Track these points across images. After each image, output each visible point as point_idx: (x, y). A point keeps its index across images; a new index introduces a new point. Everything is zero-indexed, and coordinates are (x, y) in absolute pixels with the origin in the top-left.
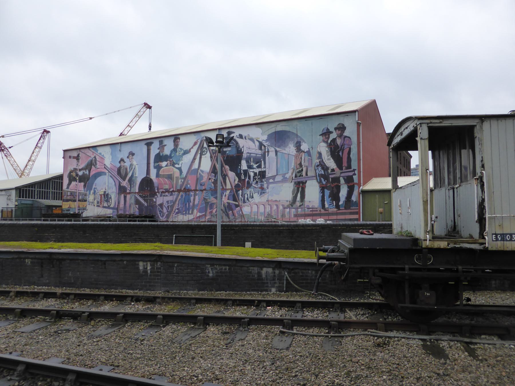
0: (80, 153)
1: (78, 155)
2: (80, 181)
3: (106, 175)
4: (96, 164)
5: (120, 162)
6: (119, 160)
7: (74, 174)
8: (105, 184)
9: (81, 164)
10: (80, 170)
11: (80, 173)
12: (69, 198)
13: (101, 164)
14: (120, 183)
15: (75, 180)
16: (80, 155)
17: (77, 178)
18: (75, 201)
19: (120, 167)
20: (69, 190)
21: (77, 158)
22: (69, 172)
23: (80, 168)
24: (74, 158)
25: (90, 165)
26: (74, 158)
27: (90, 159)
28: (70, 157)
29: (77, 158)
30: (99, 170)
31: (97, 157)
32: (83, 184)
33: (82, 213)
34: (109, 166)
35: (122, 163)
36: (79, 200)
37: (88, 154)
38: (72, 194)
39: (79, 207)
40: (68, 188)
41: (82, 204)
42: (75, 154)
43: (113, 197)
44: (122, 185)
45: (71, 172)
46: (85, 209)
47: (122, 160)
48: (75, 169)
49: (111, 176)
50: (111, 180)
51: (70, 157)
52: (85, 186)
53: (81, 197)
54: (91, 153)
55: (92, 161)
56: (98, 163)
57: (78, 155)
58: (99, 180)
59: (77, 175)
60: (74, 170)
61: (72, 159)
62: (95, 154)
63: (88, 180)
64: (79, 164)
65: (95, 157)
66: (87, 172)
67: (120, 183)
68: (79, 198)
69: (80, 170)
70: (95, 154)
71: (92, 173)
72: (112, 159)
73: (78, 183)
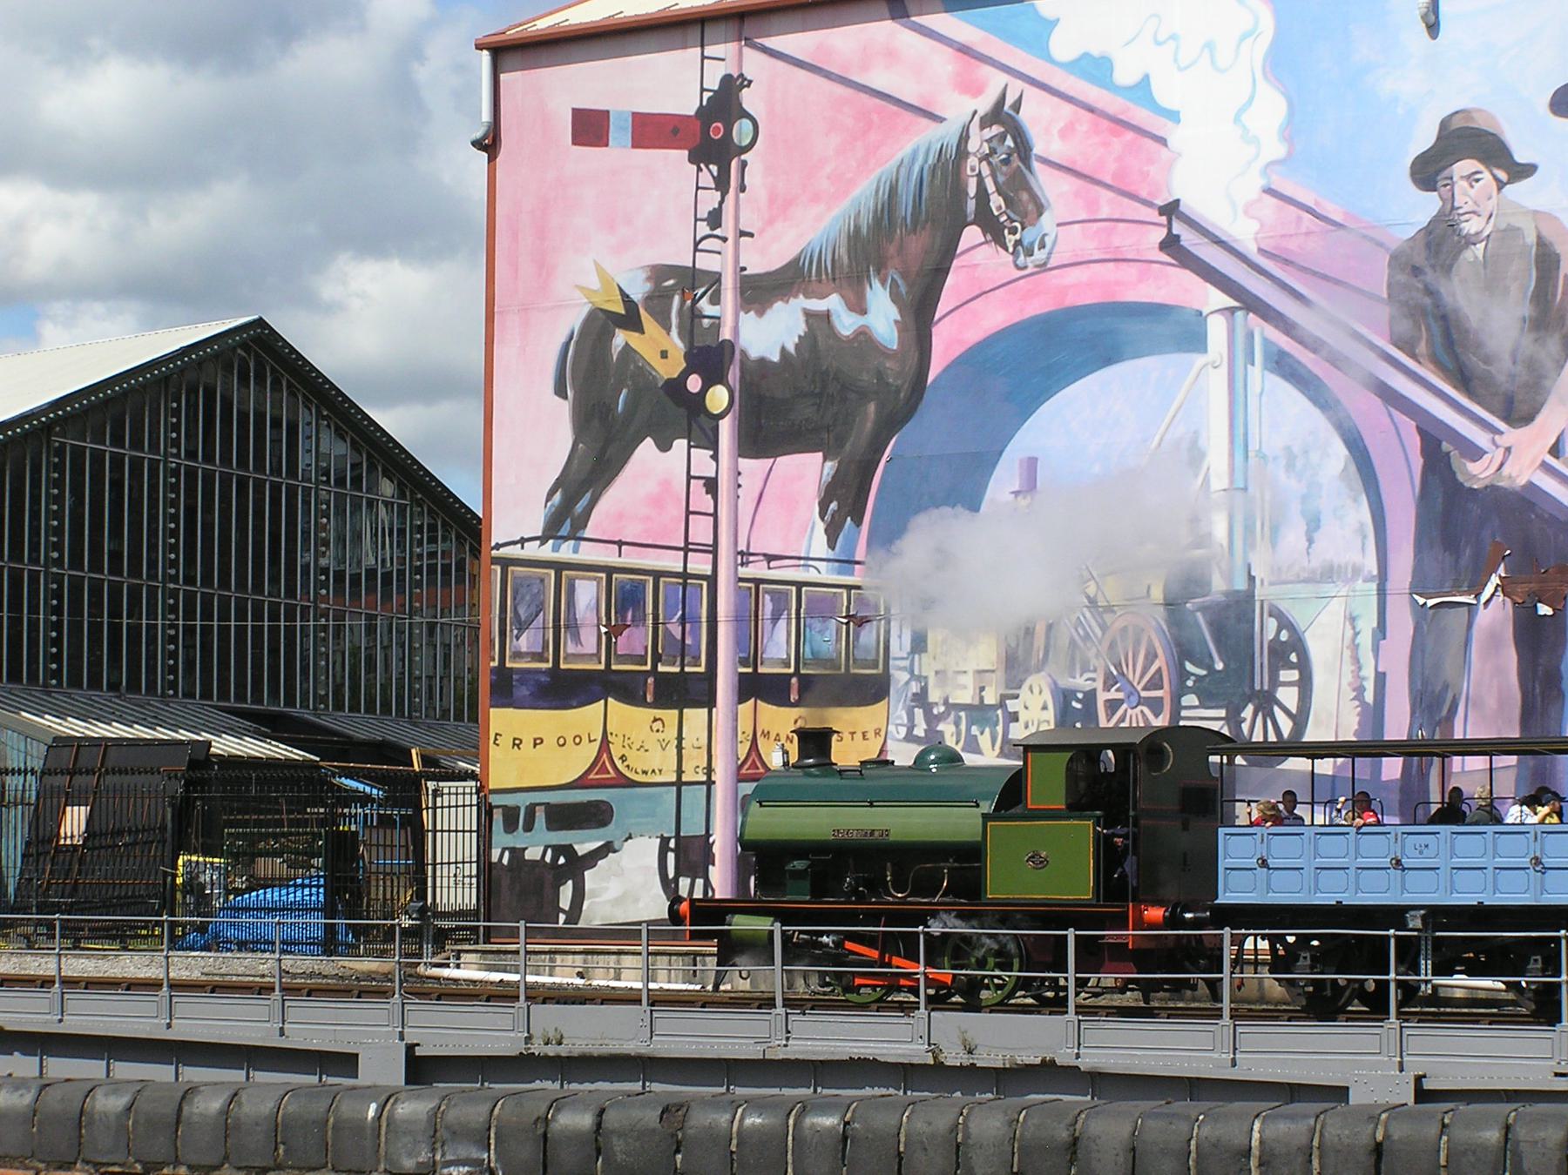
0: (754, 64)
1: (725, 101)
2: (763, 437)
3: (1191, 337)
4: (1024, 202)
5: (1428, 172)
6: (1425, 138)
7: (660, 350)
8: (1196, 456)
9: (780, 206)
10: (759, 292)
11: (769, 334)
12: (584, 649)
13: (1108, 204)
14: (1438, 451)
15: (679, 415)
16: (749, 99)
17: (718, 398)
18: (686, 691)
19: (1442, 239)
20: (589, 553)
21: (711, 136)
22: (574, 319)
23: (762, 259)
24: (652, 131)
25: (921, 227)
26: (652, 131)
27: (947, 134)
28: (590, 128)
29: (711, 136)
30: (1078, 287)
31: (1037, 115)
32: (807, 470)
34: (1245, 234)
35: (1471, 183)
36: (755, 687)
37: (879, 81)
38: (626, 596)
40: (566, 519)
42: (673, 81)
43: (1322, 647)
44: (1477, 473)
45: (600, 325)
47: (1468, 141)
48: (680, 286)
49: (1282, 365)
50: (1285, 414)
51: (590, 128)
52: (845, 500)
53: (778, 647)
54: (943, 62)
55: (950, 165)
56: (1046, 182)
57: (725, 101)
58: (1079, 423)
59: (710, 358)
60: (658, 301)
61: (619, 152)
62: (996, 81)
63: (893, 422)
64: (748, 208)
65: (1002, 116)
66: (882, 316)
67: (1438, 451)
68: (750, 654)
69: (759, 292)
70: (996, 81)
71: (950, 338)
72: (1290, 132)
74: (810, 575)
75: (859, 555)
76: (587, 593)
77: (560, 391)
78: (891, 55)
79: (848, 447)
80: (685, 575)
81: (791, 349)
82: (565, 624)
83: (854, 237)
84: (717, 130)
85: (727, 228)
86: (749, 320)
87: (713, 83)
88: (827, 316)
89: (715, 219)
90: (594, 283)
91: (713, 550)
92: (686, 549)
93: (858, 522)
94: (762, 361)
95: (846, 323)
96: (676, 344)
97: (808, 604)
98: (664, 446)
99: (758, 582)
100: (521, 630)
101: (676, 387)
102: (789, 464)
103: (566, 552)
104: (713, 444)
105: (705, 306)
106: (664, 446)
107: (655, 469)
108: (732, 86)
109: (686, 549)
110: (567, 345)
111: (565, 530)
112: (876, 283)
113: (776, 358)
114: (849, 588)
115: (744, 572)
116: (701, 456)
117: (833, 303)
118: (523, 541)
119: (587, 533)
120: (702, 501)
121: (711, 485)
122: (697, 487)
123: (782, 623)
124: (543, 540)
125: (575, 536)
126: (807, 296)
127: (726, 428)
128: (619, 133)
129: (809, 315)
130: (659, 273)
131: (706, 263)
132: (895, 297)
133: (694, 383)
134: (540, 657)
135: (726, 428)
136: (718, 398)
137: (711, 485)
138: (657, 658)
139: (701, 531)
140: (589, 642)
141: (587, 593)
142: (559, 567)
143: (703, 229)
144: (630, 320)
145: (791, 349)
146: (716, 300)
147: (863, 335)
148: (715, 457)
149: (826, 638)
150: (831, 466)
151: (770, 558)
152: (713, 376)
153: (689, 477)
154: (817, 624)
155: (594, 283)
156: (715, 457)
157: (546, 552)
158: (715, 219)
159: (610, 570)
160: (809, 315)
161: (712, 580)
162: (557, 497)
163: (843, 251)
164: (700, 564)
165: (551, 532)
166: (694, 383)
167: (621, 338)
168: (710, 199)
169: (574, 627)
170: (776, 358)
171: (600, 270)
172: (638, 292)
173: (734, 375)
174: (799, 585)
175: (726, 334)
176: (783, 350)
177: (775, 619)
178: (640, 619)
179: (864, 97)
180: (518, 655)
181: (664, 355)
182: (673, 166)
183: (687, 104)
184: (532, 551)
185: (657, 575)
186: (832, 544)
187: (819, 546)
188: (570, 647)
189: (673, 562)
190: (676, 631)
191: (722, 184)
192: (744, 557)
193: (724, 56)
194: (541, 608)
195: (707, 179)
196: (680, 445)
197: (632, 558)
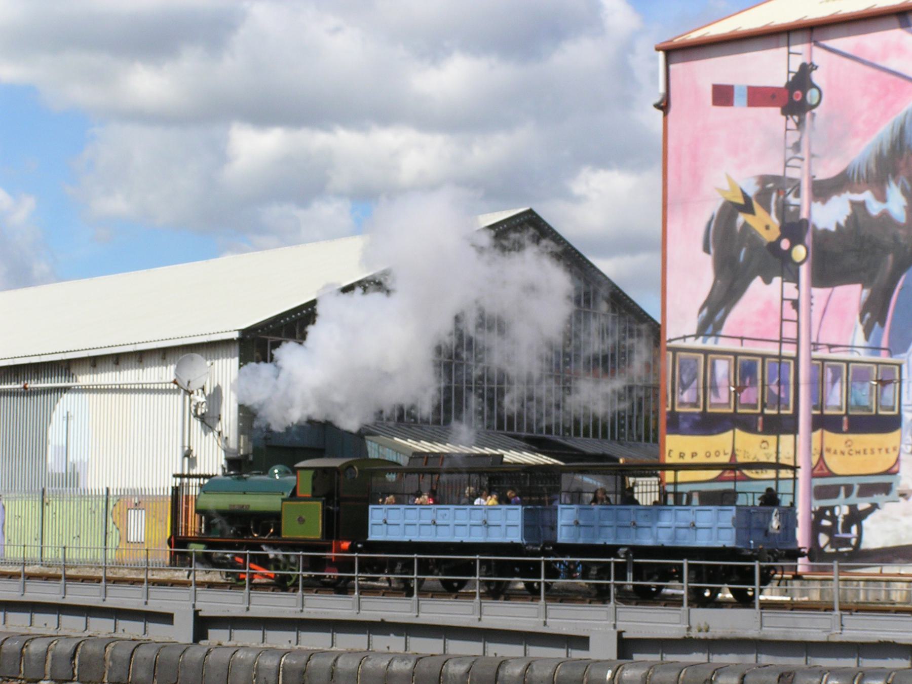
0: (819, 56)
1: (802, 79)
2: (825, 275)
7: (765, 225)
11: (829, 215)
12: (721, 400)
15: (776, 263)
16: (817, 77)
17: (799, 253)
18: (782, 425)
20: (724, 344)
22: (713, 207)
23: (827, 170)
24: (759, 97)
26: (759, 97)
28: (723, 95)
29: (795, 98)
32: (852, 295)
33: (856, 517)
37: (893, 64)
38: (746, 370)
39: (820, 470)
40: (710, 323)
41: (853, 456)
42: (772, 67)
45: (729, 211)
46: (880, 487)
48: (773, 188)
51: (723, 95)
52: (874, 311)
57: (802, 79)
59: (794, 229)
60: (764, 196)
61: (740, 109)
68: (819, 402)
69: (823, 190)
73: (803, 287)
74: (854, 356)
75: (884, 344)
76: (722, 368)
77: (706, 249)
78: (900, 49)
79: (876, 281)
80: (780, 357)
81: (842, 223)
82: (710, 386)
83: (880, 159)
84: (797, 95)
85: (804, 153)
86: (817, 207)
87: (795, 68)
88: (862, 204)
89: (797, 147)
90: (726, 186)
91: (797, 342)
92: (781, 341)
93: (883, 324)
94: (826, 231)
95: (875, 208)
96: (774, 221)
97: (856, 374)
98: (768, 281)
99: (823, 360)
100: (684, 387)
101: (774, 246)
102: (842, 291)
103: (710, 344)
104: (796, 279)
105: (792, 199)
106: (768, 281)
107: (762, 295)
108: (806, 70)
109: (781, 341)
110: (710, 223)
111: (710, 330)
112: (893, 184)
113: (833, 228)
114: (877, 364)
115: (815, 355)
116: (790, 287)
117: (866, 196)
118: (685, 337)
119: (724, 332)
120: (790, 313)
121: (796, 304)
122: (787, 305)
123: (838, 385)
124: (697, 336)
125: (716, 334)
126: (852, 192)
127: (804, 271)
128: (740, 98)
129: (853, 204)
130: (764, 180)
131: (792, 173)
132: (904, 192)
133: (785, 244)
134: (695, 405)
135: (804, 271)
136: (799, 253)
137: (796, 304)
138: (764, 406)
139: (790, 331)
140: (724, 396)
141: (722, 368)
142: (706, 352)
143: (790, 153)
144: (747, 207)
145: (842, 223)
146: (797, 195)
147: (885, 215)
148: (798, 287)
149: (865, 395)
150: (866, 293)
151: (830, 346)
152: (796, 239)
153: (783, 299)
154: (858, 385)
155: (726, 186)
156: (798, 287)
157: (698, 343)
158: (797, 147)
159: (736, 354)
160: (853, 204)
161: (796, 360)
162: (705, 312)
163: (873, 166)
164: (789, 350)
165: (702, 332)
166: (785, 244)
167: (741, 218)
168: (793, 137)
169: (715, 388)
170: (833, 228)
171: (729, 178)
172: (751, 191)
173: (808, 239)
174: (848, 362)
175: (804, 215)
176: (838, 225)
177: (834, 382)
178: (753, 383)
179: (885, 75)
180: (682, 404)
181: (767, 227)
182: (772, 115)
183: (778, 79)
184: (691, 343)
185: (764, 357)
186: (867, 337)
187: (859, 338)
188: (712, 399)
189: (772, 349)
190: (775, 389)
191: (800, 125)
192: (815, 346)
193: (802, 52)
194: (695, 376)
195: (792, 124)
196: (777, 280)
197: (749, 347)
